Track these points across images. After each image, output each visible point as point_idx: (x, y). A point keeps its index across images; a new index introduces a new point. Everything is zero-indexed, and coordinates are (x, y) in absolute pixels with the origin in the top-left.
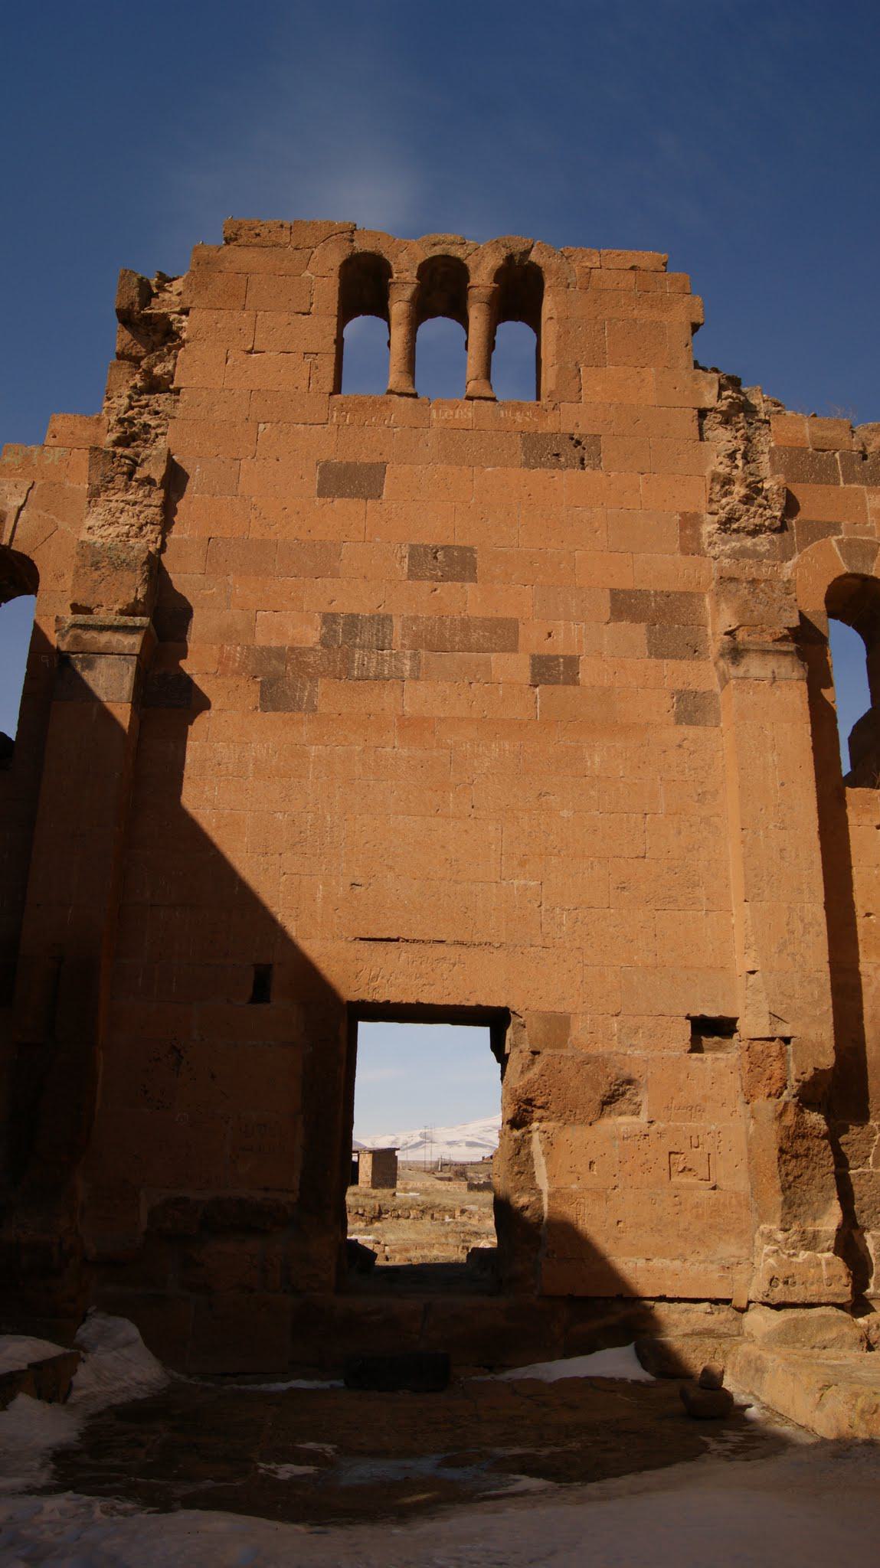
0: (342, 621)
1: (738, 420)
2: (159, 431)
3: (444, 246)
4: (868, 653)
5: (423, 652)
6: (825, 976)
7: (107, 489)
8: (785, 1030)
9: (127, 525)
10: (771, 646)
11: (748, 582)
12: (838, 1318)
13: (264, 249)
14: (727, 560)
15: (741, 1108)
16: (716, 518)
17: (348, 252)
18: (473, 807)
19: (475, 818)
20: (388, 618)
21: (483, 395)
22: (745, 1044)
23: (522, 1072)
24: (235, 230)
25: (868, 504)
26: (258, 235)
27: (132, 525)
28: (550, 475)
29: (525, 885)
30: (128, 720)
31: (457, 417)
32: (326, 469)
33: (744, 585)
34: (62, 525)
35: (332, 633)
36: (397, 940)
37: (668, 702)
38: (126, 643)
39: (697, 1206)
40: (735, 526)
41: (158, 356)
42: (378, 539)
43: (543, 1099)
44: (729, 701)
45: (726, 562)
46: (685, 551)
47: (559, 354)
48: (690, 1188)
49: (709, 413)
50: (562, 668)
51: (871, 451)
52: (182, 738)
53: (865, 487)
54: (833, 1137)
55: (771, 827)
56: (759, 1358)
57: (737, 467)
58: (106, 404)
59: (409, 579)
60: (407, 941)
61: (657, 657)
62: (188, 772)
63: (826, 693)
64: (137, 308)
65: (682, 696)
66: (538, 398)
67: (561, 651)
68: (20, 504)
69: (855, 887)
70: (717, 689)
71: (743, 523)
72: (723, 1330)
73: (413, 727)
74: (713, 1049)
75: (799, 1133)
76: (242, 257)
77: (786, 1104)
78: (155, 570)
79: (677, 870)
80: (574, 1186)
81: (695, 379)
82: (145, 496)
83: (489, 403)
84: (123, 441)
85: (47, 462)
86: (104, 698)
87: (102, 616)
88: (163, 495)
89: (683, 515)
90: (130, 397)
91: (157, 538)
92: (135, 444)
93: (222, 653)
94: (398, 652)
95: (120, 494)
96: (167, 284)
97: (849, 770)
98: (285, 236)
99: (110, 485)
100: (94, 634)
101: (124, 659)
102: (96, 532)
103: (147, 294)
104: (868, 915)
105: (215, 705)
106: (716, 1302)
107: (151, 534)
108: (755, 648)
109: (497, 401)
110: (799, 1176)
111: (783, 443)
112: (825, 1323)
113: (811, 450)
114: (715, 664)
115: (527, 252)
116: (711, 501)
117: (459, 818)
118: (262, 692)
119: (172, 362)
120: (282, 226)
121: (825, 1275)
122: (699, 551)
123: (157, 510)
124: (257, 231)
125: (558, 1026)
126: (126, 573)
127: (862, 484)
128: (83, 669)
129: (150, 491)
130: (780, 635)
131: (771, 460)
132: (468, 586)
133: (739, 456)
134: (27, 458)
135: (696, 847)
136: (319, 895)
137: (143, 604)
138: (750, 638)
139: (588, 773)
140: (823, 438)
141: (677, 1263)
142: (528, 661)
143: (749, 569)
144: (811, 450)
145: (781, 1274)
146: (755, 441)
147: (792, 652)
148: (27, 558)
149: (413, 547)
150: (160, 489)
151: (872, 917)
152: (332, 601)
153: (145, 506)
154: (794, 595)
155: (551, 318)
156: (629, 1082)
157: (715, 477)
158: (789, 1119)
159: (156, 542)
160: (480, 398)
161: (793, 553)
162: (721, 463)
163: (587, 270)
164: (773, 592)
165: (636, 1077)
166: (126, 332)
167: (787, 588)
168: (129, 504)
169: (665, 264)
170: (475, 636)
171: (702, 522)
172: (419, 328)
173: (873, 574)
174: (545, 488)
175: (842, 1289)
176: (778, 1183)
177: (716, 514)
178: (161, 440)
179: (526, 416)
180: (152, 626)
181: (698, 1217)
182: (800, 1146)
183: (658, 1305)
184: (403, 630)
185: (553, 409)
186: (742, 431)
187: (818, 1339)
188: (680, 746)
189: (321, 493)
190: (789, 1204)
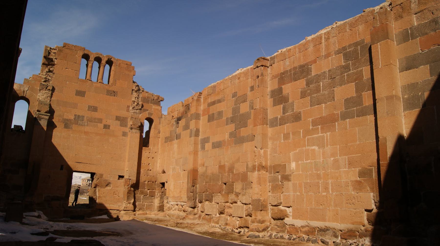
0: (77, 116)
5: (89, 122)
6: (136, 172)
10: (136, 128)
15: (123, 187)
16: (132, 107)
17: (84, 53)
20: (84, 116)
22: (125, 179)
23: (96, 181)
34: (34, 94)
36: (81, 163)
40: (134, 108)
43: (99, 185)
44: (129, 134)
45: (132, 113)
46: (127, 111)
52: (53, 131)
53: (153, 105)
54: (134, 191)
56: (123, 215)
62: (53, 136)
63: (142, 134)
64: (48, 56)
67: (108, 124)
72: (118, 213)
73: (86, 133)
74: (121, 179)
75: (130, 190)
77: (129, 187)
78: (50, 105)
80: (101, 196)
82: (48, 92)
83: (103, 84)
84: (45, 81)
85: (32, 83)
86: (42, 125)
89: (128, 106)
90: (46, 73)
92: (47, 82)
95: (44, 91)
97: (145, 137)
99: (43, 89)
105: (57, 127)
107: (49, 98)
112: (130, 212)
115: (111, 58)
116: (132, 104)
118: (65, 126)
121: (131, 207)
123: (50, 94)
125: (101, 175)
129: (49, 91)
131: (141, 99)
132: (96, 113)
133: (137, 98)
141: (113, 205)
142: (103, 125)
148: (28, 99)
155: (113, 70)
156: (110, 183)
157: (133, 101)
158: (129, 189)
160: (101, 83)
165: (111, 182)
173: (151, 118)
175: (133, 209)
176: (127, 196)
178: (51, 82)
181: (116, 200)
182: (130, 192)
183: (110, 210)
186: (138, 94)
187: (129, 214)
188: (122, 139)
189: (76, 95)
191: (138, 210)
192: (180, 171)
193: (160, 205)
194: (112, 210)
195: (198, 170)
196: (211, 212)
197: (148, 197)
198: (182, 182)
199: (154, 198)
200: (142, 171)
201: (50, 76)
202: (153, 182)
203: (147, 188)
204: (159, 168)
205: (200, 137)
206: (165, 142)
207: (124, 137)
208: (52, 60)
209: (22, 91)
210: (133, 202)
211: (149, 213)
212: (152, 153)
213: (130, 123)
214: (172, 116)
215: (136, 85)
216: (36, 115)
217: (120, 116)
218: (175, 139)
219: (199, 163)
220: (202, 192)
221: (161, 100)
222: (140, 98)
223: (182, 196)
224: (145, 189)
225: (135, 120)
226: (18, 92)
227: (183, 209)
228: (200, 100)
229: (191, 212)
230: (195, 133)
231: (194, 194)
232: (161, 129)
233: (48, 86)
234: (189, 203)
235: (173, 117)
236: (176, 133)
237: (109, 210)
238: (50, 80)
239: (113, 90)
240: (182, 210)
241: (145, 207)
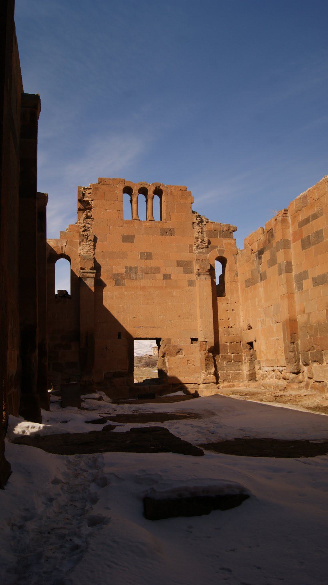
2: (91, 228)
3: (143, 185)
4: (222, 267)
5: (144, 274)
6: (213, 331)
7: (83, 242)
8: (206, 340)
10: (205, 273)
12: (214, 385)
14: (197, 254)
15: (199, 353)
16: (196, 245)
17: (124, 186)
22: (200, 342)
23: (164, 348)
26: (105, 182)
34: (74, 249)
39: (192, 369)
40: (199, 247)
44: (197, 283)
45: (197, 254)
46: (190, 252)
48: (191, 366)
54: (214, 357)
56: (202, 390)
62: (104, 298)
63: (214, 280)
70: (195, 280)
71: (200, 247)
72: (196, 388)
73: (143, 288)
75: (208, 357)
77: (206, 352)
78: (94, 259)
80: (173, 367)
81: (192, 215)
84: (84, 231)
85: (69, 235)
86: (89, 286)
89: (190, 245)
90: (84, 220)
99: (83, 241)
104: (220, 320)
105: (107, 285)
106: (195, 383)
107: (92, 251)
110: (208, 363)
115: (160, 186)
116: (195, 242)
118: (115, 282)
121: (212, 378)
122: (193, 252)
123: (93, 246)
128: (85, 280)
129: (91, 242)
131: (206, 233)
133: (200, 233)
141: (189, 378)
142: (162, 275)
145: (205, 379)
156: (181, 349)
158: (207, 355)
160: (152, 221)
161: (209, 252)
165: (182, 348)
170: (153, 270)
171: (193, 246)
173: (223, 256)
175: (215, 381)
176: (205, 365)
182: (208, 359)
189: (123, 242)
190: (206, 368)
191: (222, 381)
192: (271, 325)
193: (251, 372)
194: (188, 384)
195: (296, 320)
196: (323, 378)
197: (233, 363)
198: (277, 338)
199: (242, 364)
200: (221, 329)
201: (89, 223)
202: (237, 343)
203: (229, 351)
204: (243, 323)
205: (293, 272)
206: (247, 286)
207: (190, 287)
208: (88, 203)
209: (60, 247)
210: (214, 372)
211: (237, 384)
212: (231, 303)
213: (196, 267)
214: (251, 250)
215: (197, 216)
216: (80, 274)
217: (182, 260)
218: (259, 281)
219: (296, 310)
220: (307, 350)
221: (233, 230)
222: (205, 233)
223: (279, 358)
224: (228, 353)
225: (202, 262)
226: (55, 249)
227: (282, 376)
228: (286, 220)
229: (293, 379)
230: (286, 268)
231: (295, 354)
232: (238, 270)
233: (89, 236)
234: (290, 367)
235: (252, 250)
236: (259, 272)
237: (185, 384)
238: (89, 228)
240: (282, 378)
241: (231, 377)
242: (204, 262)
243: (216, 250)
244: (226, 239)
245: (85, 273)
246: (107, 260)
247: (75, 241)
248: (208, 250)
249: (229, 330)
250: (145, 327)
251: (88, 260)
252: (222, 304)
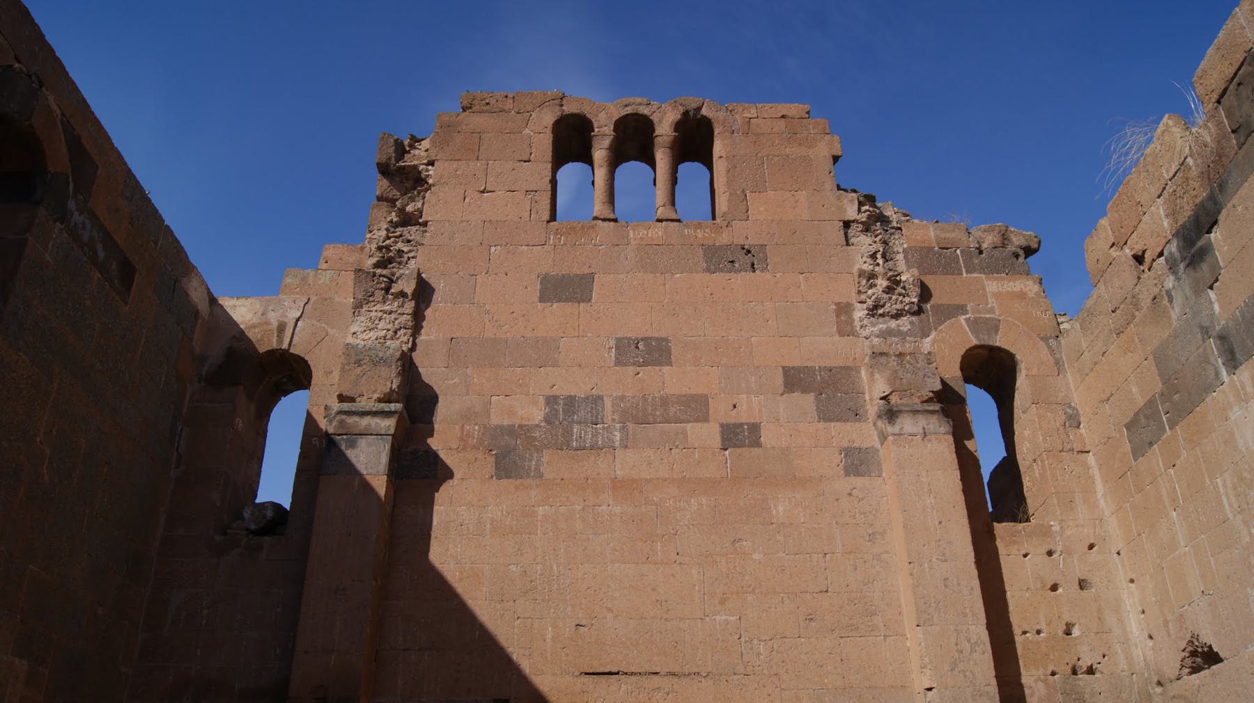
0: (561, 402)
1: (876, 228)
2: (411, 255)
4: (999, 410)
5: (631, 426)
9: (384, 330)
10: (920, 407)
11: (896, 356)
13: (494, 114)
14: (878, 339)
16: (865, 306)
17: (559, 114)
18: (678, 554)
19: (680, 563)
20: (601, 398)
21: (669, 218)
24: (469, 101)
25: (987, 289)
26: (488, 104)
27: (388, 330)
28: (727, 277)
29: (726, 620)
30: (384, 489)
31: (649, 235)
32: (545, 280)
33: (893, 358)
35: (553, 412)
37: (837, 458)
38: (382, 425)
40: (881, 311)
41: (410, 197)
42: (589, 335)
44: (889, 455)
45: (876, 341)
46: (841, 333)
47: (729, 184)
49: (852, 224)
50: (746, 434)
51: (986, 247)
52: (431, 503)
53: (983, 276)
55: (934, 560)
57: (878, 265)
58: (368, 236)
59: (616, 366)
60: (626, 674)
61: (825, 421)
64: (393, 161)
65: (848, 452)
66: (714, 218)
68: (298, 316)
69: (1011, 609)
70: (878, 446)
71: (887, 308)
73: (624, 487)
76: (476, 121)
78: (407, 366)
79: (856, 601)
81: (839, 198)
83: (675, 224)
84: (382, 264)
86: (364, 472)
87: (364, 404)
88: (413, 305)
89: (838, 304)
90: (387, 230)
91: (409, 340)
92: (391, 266)
93: (462, 434)
94: (609, 426)
95: (379, 305)
96: (417, 144)
98: (509, 104)
99: (371, 299)
100: (357, 419)
101: (381, 439)
102: (359, 337)
103: (401, 151)
104: (1025, 633)
107: (404, 336)
108: (907, 409)
109: (682, 222)
111: (913, 245)
113: (936, 248)
114: (875, 424)
115: (699, 109)
116: (859, 292)
117: (666, 564)
118: (496, 463)
119: (421, 201)
120: (506, 97)
122: (853, 333)
124: (487, 101)
126: (383, 368)
127: (981, 273)
128: (347, 449)
129: (403, 303)
130: (927, 398)
132: (666, 369)
133: (879, 256)
134: (304, 279)
135: (871, 581)
136: (549, 636)
137: (397, 393)
138: (902, 401)
139: (774, 521)
140: (945, 239)
142: (717, 429)
143: (895, 345)
144: (936, 248)
146: (891, 244)
147: (937, 411)
148: (303, 359)
149: (619, 340)
150: (411, 300)
151: (1027, 635)
152: (554, 386)
153: (399, 314)
154: (934, 364)
155: (721, 157)
157: (861, 274)
159: (408, 343)
160: (667, 220)
161: (930, 330)
162: (865, 262)
163: (748, 120)
164: (918, 363)
166: (385, 180)
167: (929, 359)
168: (386, 313)
169: (808, 113)
171: (854, 310)
172: (617, 170)
173: (998, 344)
174: (724, 289)
177: (865, 303)
178: (412, 262)
179: (705, 232)
180: (404, 411)
184: (612, 407)
185: (727, 226)
186: (880, 237)
188: (850, 494)
189: (542, 299)
204: (1150, 643)
207: (858, 482)
209: (275, 324)
212: (1067, 552)
215: (861, 199)
217: (809, 364)
218: (1217, 374)
221: (1023, 243)
222: (900, 257)
225: (901, 364)
232: (1077, 400)
233: (398, 278)
239: (742, 243)
242: (908, 362)
243: (961, 326)
244: (997, 279)
245: (350, 413)
246: (469, 371)
247: (338, 302)
248: (921, 321)
249: (1081, 683)
250: (632, 674)
251: (378, 362)
252: (1025, 556)
